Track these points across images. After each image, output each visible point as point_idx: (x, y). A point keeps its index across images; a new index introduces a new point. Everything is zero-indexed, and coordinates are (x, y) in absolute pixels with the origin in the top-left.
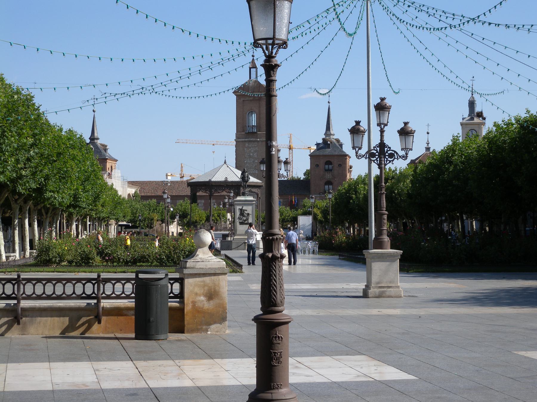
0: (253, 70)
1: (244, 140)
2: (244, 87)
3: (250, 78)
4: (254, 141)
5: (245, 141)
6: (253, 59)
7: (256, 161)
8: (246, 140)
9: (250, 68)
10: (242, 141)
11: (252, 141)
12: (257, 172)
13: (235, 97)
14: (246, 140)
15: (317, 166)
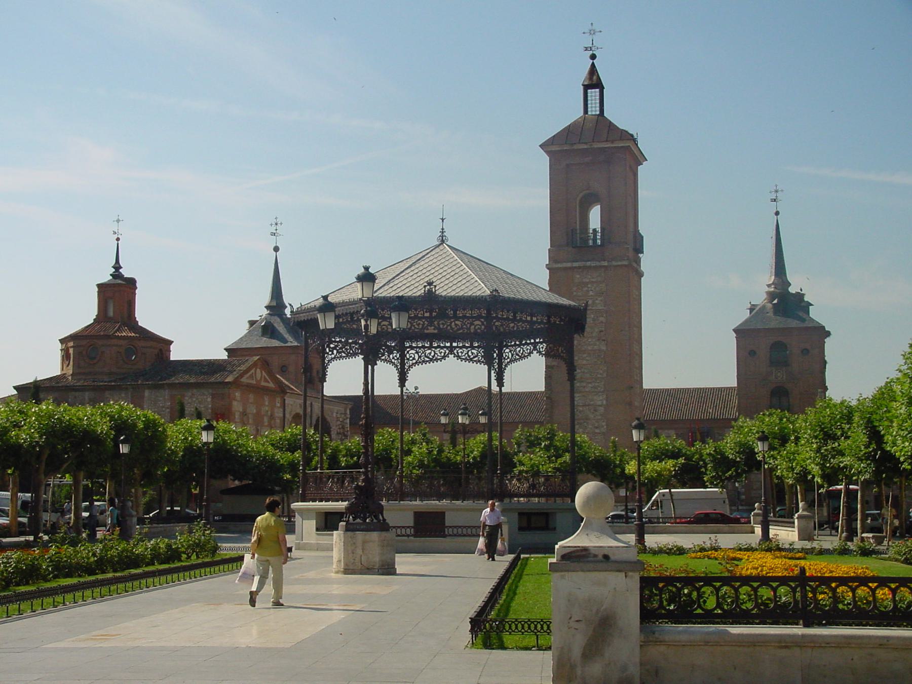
0: (594, 93)
1: (569, 265)
2: (569, 134)
3: (586, 111)
4: (596, 268)
5: (572, 269)
6: (593, 65)
7: (601, 319)
8: (576, 264)
9: (586, 88)
10: (566, 269)
11: (590, 267)
12: (604, 348)
13: (545, 160)
14: (576, 264)
15: (752, 353)
